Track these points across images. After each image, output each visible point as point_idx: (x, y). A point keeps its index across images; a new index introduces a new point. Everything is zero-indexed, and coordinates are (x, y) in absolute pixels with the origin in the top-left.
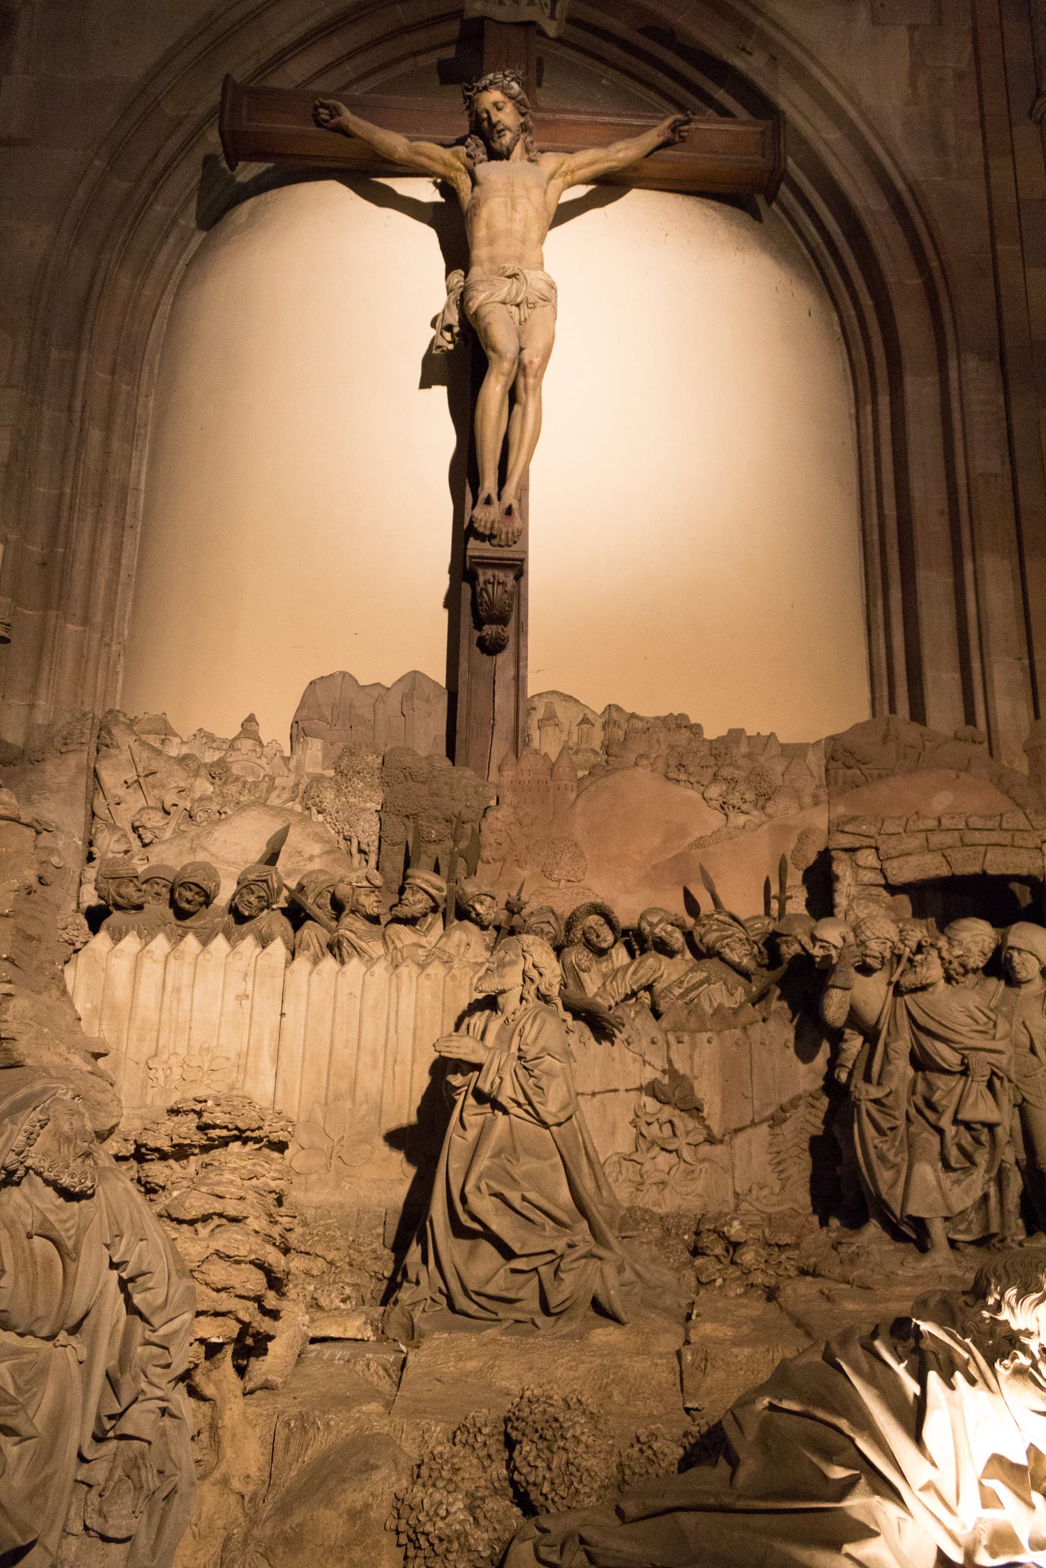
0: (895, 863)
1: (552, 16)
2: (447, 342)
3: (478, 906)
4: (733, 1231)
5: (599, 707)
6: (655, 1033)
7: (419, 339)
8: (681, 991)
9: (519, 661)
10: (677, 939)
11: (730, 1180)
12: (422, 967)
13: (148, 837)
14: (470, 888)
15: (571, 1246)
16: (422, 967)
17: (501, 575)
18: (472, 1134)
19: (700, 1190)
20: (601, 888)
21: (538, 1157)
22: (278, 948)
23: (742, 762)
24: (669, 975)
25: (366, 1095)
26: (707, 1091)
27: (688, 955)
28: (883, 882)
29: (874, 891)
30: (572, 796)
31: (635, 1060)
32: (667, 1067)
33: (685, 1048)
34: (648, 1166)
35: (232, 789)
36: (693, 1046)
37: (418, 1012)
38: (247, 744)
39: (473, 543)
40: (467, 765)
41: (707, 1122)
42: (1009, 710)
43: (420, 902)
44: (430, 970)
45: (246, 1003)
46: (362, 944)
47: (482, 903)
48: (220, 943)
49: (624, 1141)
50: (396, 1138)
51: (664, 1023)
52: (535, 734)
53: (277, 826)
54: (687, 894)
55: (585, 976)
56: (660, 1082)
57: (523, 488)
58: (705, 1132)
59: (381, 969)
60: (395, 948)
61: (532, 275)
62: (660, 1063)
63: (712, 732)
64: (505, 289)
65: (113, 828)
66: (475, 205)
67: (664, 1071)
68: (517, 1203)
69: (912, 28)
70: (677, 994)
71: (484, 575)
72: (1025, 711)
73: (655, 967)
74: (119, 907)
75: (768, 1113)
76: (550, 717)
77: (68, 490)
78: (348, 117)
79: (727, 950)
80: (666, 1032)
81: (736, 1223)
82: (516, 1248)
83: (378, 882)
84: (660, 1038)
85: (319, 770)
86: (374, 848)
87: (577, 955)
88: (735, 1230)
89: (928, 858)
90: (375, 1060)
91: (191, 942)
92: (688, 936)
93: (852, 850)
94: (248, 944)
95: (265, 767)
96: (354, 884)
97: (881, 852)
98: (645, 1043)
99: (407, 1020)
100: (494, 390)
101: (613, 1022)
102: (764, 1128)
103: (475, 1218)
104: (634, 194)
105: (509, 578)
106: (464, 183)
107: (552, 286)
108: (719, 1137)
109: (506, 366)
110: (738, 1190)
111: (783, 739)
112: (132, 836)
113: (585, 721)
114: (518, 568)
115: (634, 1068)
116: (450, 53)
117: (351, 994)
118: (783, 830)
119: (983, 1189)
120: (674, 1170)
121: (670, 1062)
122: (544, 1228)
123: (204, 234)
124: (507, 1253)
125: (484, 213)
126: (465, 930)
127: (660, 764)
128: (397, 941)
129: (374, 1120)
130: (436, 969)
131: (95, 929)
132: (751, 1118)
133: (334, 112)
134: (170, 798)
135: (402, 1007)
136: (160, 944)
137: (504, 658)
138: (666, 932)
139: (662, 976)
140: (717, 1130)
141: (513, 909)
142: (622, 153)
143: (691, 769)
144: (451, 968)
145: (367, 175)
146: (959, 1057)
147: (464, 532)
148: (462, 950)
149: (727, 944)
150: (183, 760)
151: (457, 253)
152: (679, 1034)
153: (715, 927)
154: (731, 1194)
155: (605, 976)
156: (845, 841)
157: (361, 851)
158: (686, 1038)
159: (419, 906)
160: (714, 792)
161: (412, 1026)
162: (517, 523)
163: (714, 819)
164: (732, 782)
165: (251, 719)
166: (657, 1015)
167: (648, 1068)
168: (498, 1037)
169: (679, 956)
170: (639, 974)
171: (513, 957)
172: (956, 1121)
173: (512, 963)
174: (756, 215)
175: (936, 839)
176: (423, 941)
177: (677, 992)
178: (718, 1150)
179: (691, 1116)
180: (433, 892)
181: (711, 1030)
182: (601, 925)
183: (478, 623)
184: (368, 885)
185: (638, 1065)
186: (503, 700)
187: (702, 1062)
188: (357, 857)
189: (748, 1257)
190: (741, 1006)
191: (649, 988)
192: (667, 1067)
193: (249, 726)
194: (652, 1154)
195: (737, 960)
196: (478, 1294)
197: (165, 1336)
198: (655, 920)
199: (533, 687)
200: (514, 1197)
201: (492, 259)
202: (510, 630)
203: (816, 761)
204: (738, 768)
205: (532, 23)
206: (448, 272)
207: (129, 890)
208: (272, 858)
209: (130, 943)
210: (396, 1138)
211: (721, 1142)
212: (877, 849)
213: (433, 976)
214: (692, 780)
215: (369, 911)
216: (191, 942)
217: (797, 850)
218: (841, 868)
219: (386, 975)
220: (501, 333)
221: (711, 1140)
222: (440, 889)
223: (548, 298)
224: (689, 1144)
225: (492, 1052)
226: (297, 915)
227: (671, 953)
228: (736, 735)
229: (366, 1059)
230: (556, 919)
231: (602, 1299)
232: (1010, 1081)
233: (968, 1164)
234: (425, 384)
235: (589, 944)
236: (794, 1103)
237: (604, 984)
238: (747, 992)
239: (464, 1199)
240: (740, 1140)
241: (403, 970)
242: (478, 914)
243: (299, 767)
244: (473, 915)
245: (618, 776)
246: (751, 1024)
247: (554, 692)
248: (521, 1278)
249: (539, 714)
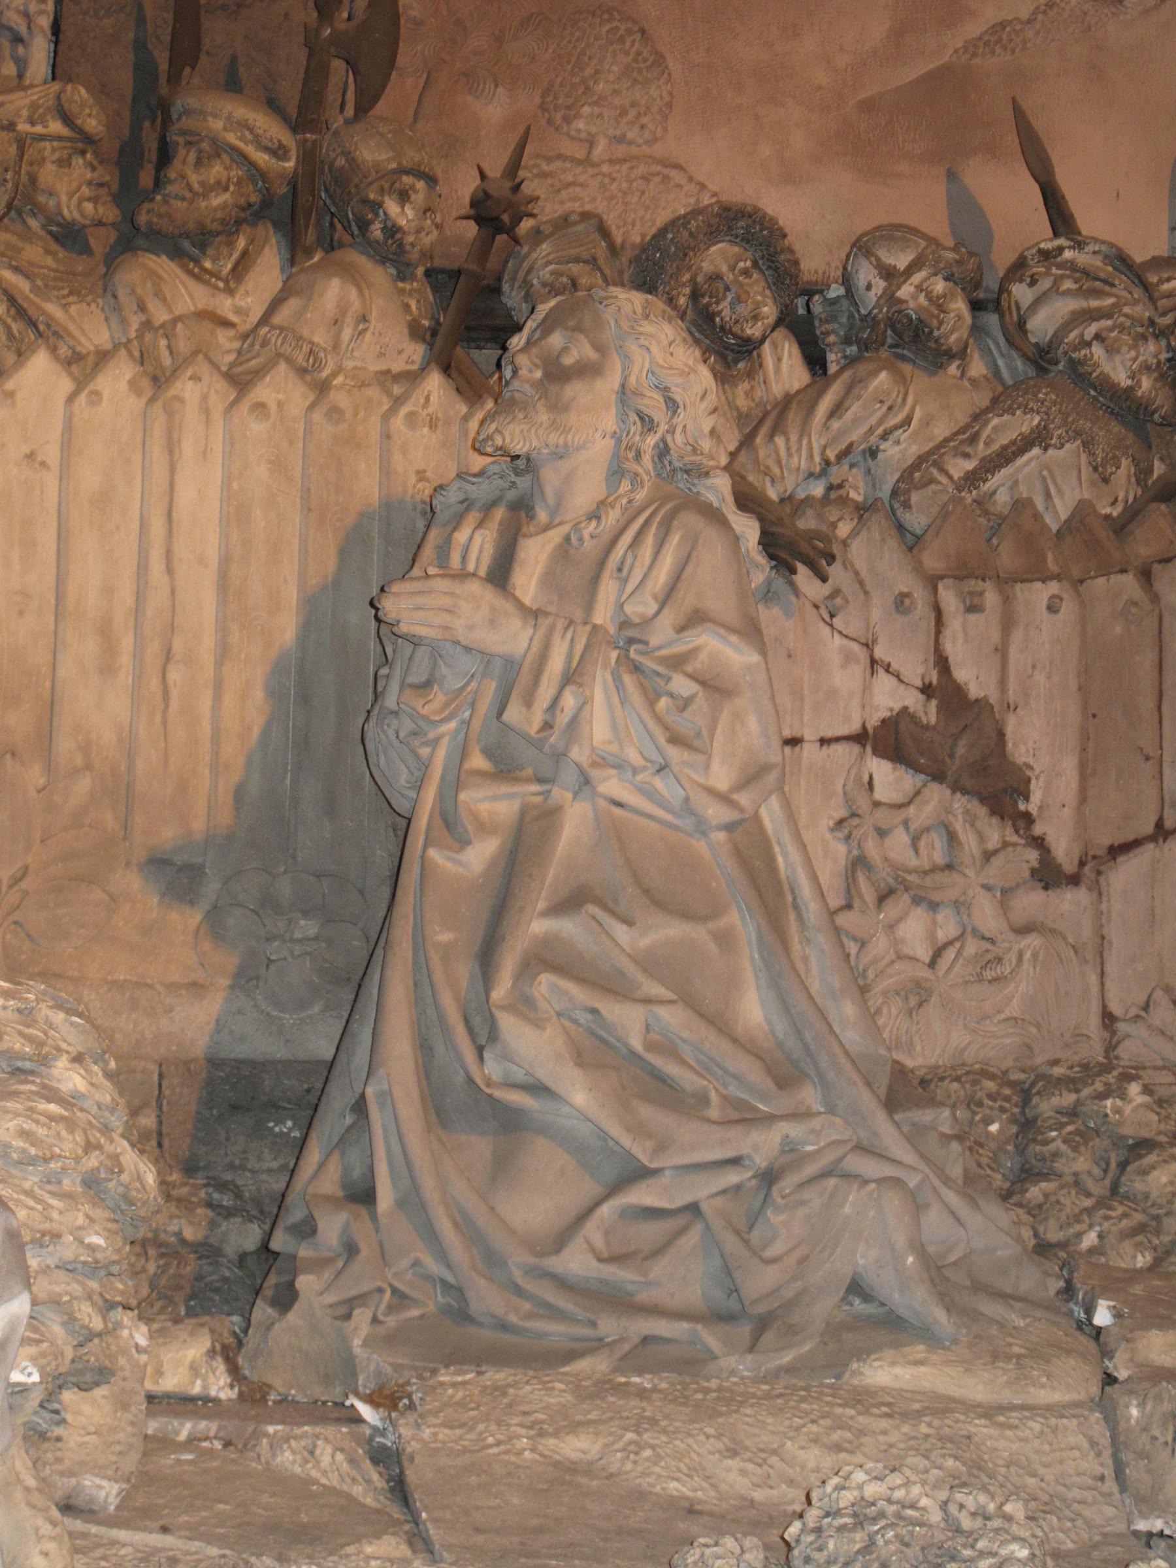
3: (392, 207)
6: (905, 582)
8: (969, 465)
11: (1093, 979)
12: (241, 381)
14: (372, 152)
16: (241, 381)
18: (480, 854)
19: (1014, 1008)
20: (716, 166)
21: (686, 915)
24: (927, 422)
25: (86, 749)
26: (1040, 742)
31: (848, 658)
32: (934, 677)
36: (1008, 623)
37: (236, 513)
41: (1038, 829)
44: (264, 392)
46: (53, 309)
47: (404, 197)
50: (177, 875)
56: (913, 718)
58: (1033, 856)
59: (117, 382)
60: (147, 325)
62: (915, 666)
67: (927, 690)
70: (957, 475)
79: (1097, 351)
80: (933, 582)
83: (92, 124)
84: (920, 595)
90: (109, 649)
96: (23, 127)
99: (201, 537)
101: (804, 546)
108: (1069, 867)
110: (1116, 1008)
115: (846, 678)
117: (31, 456)
120: (950, 954)
121: (943, 663)
126: (350, 273)
128: (152, 305)
129: (110, 820)
130: (279, 389)
132: (1153, 820)
135: (186, 496)
138: (929, 297)
139: (908, 421)
140: (1064, 850)
141: (495, 215)
144: (322, 388)
149: (1098, 337)
152: (972, 584)
153: (1068, 285)
158: (991, 598)
159: (217, 200)
161: (213, 555)
167: (884, 681)
168: (549, 579)
169: (953, 369)
170: (849, 415)
171: (591, 354)
173: (587, 371)
176: (225, 306)
177: (960, 467)
181: (1058, 577)
182: (746, 272)
184: (65, 131)
185: (858, 670)
190: (1133, 513)
192: (934, 677)
194: (892, 909)
195: (1122, 378)
198: (901, 261)
211: (1074, 880)
213: (273, 408)
215: (70, 212)
219: (135, 404)
221: (1048, 875)
222: (279, 152)
225: (545, 623)
229: (83, 648)
230: (613, 250)
237: (747, 441)
238: (1142, 473)
240: (1125, 875)
241: (187, 390)
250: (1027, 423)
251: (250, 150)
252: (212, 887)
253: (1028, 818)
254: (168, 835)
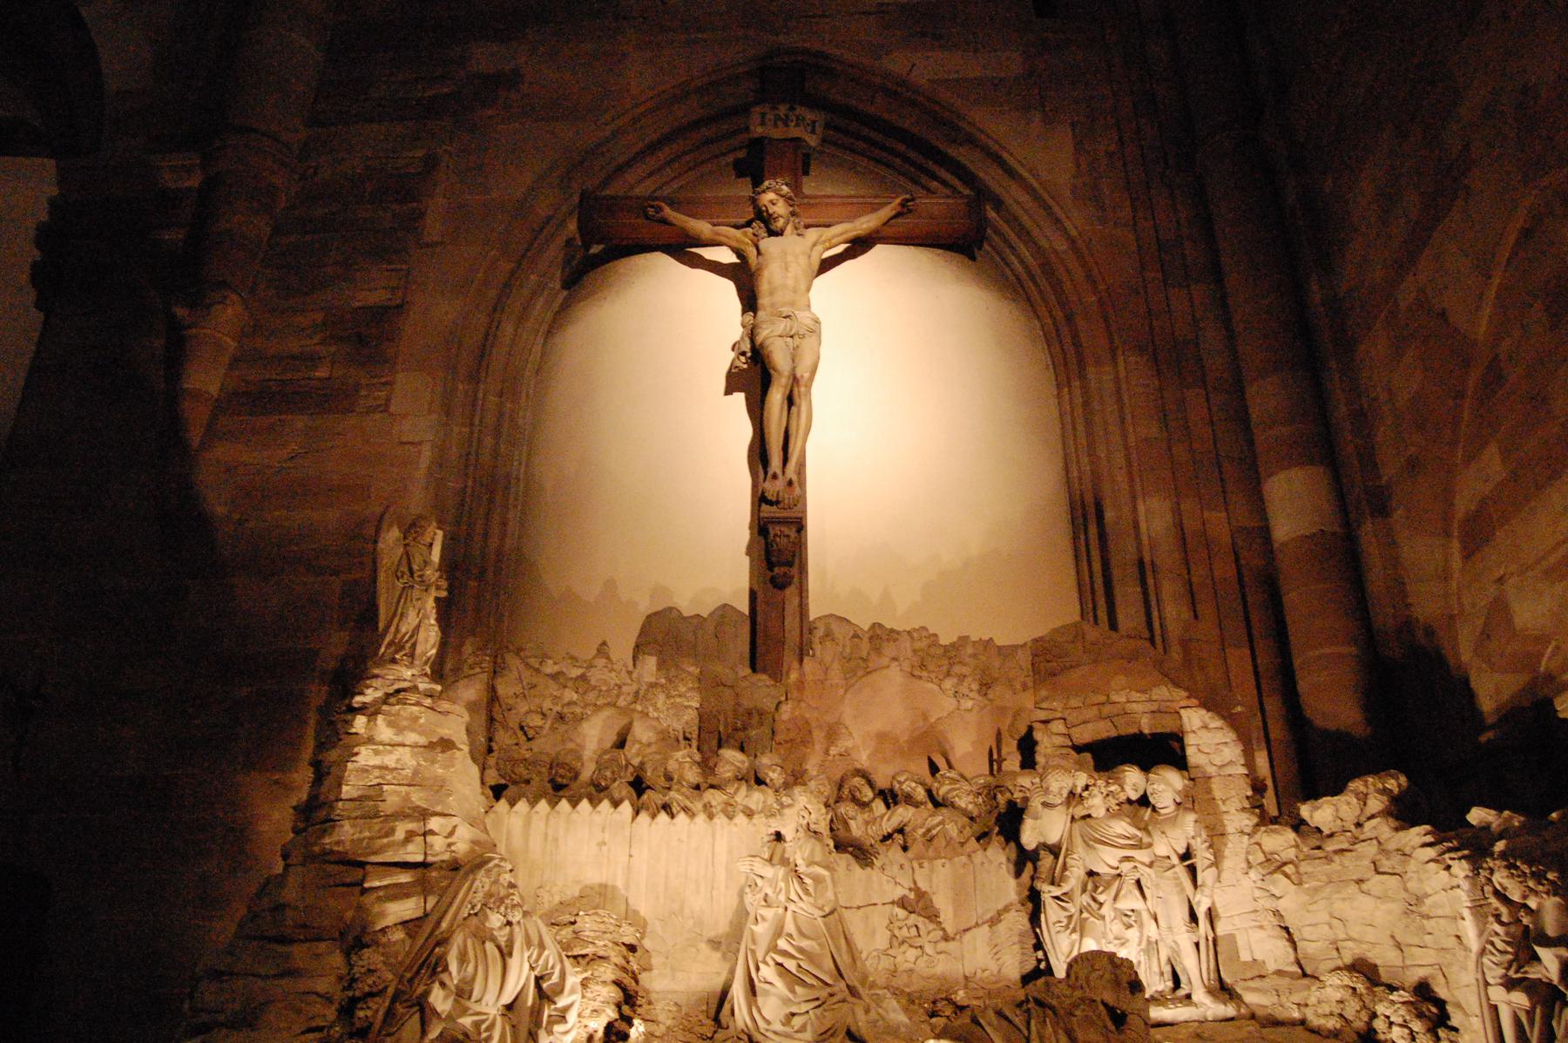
1: (813, 132)
2: (742, 363)
5: (866, 628)
7: (725, 359)
9: (802, 592)
10: (920, 794)
13: (531, 733)
15: (831, 995)
17: (786, 531)
22: (626, 808)
23: (967, 660)
26: (942, 902)
27: (930, 805)
29: (1064, 751)
30: (842, 691)
33: (925, 871)
34: (900, 959)
35: (591, 696)
36: (932, 870)
38: (601, 662)
39: (764, 507)
40: (764, 671)
42: (1173, 612)
44: (736, 820)
45: (604, 848)
48: (585, 804)
49: (881, 940)
50: (715, 944)
51: (910, 854)
52: (817, 647)
53: (625, 721)
54: (930, 760)
55: (852, 823)
57: (801, 466)
59: (701, 818)
61: (803, 316)
63: (945, 640)
64: (782, 326)
65: (506, 727)
66: (760, 269)
69: (1073, 125)
71: (774, 530)
72: (1186, 615)
73: (903, 813)
74: (515, 783)
75: (988, 917)
76: (828, 635)
77: (470, 483)
78: (668, 212)
80: (911, 861)
81: (961, 993)
85: (653, 680)
86: (695, 736)
87: (846, 809)
88: (960, 996)
89: (1102, 724)
91: (564, 805)
92: (929, 792)
93: (1046, 722)
94: (605, 805)
95: (613, 678)
98: (896, 868)
100: (776, 397)
102: (986, 928)
104: (879, 247)
105: (793, 534)
106: (751, 252)
107: (817, 322)
109: (784, 381)
111: (999, 642)
112: (520, 733)
113: (856, 636)
114: (800, 525)
115: (888, 887)
116: (741, 154)
118: (1002, 710)
123: (565, 293)
125: (766, 274)
127: (906, 666)
131: (497, 797)
133: (661, 209)
134: (547, 705)
136: (543, 805)
137: (791, 592)
140: (950, 931)
142: (865, 224)
143: (931, 668)
145: (683, 249)
147: (760, 499)
150: (555, 677)
151: (750, 302)
155: (867, 823)
156: (1043, 715)
157: (686, 739)
158: (926, 864)
160: (948, 684)
162: (797, 491)
163: (949, 703)
164: (962, 677)
165: (604, 643)
166: (905, 848)
173: (789, 806)
174: (973, 258)
175: (1106, 710)
178: (951, 946)
183: (770, 565)
185: (892, 885)
186: (791, 623)
187: (938, 879)
188: (683, 742)
191: (901, 831)
193: (602, 649)
199: (814, 612)
201: (773, 305)
202: (794, 571)
203: (1024, 658)
204: (965, 665)
205: (798, 139)
206: (744, 312)
207: (521, 770)
208: (621, 744)
209: (522, 806)
210: (715, 944)
216: (564, 805)
217: (1012, 724)
218: (1038, 735)
220: (780, 358)
221: (946, 938)
223: (815, 329)
226: (639, 786)
227: (917, 805)
228: (964, 640)
231: (853, 1029)
234: (728, 392)
235: (854, 800)
236: (1006, 909)
240: (968, 935)
241: (716, 820)
243: (640, 675)
245: (875, 675)
247: (831, 615)
249: (820, 633)
252: (723, 947)
254: (712, 934)
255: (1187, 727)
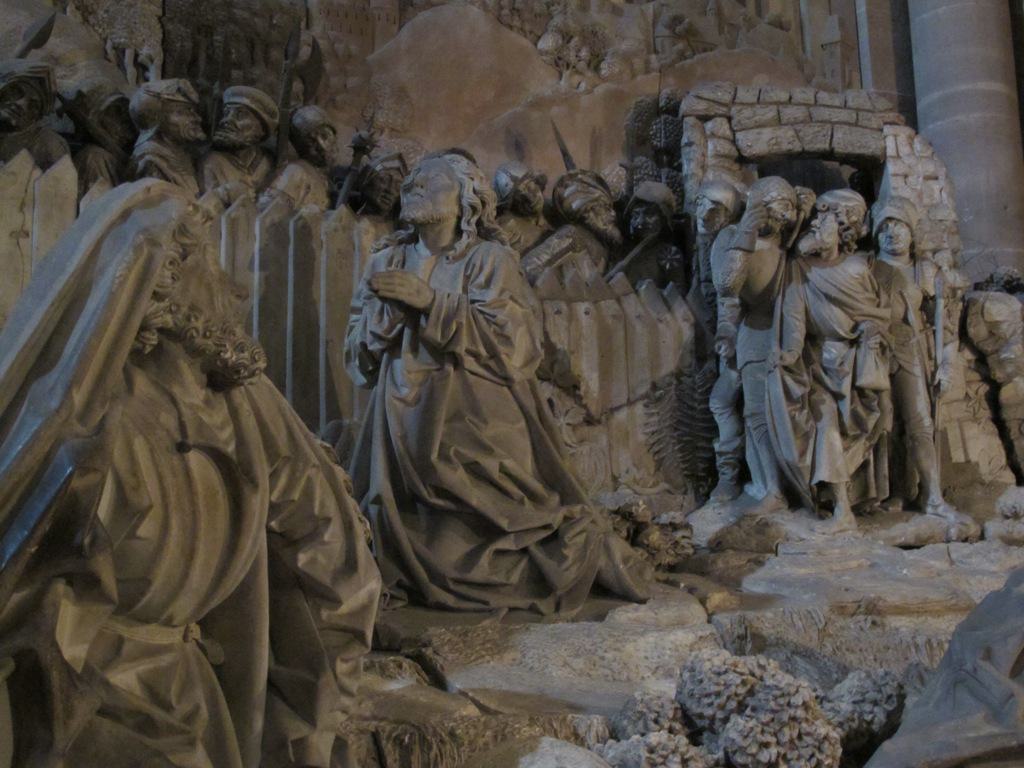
0: (752, 135)
3: (321, 141)
4: (640, 510)
11: (608, 461)
28: (736, 154)
41: (584, 402)
43: (248, 127)
58: (584, 411)
68: (496, 475)
79: (592, 214)
82: (504, 524)
97: (734, 122)
103: (442, 492)
119: (864, 456)
122: (521, 502)
124: (485, 530)
140: (594, 409)
146: (852, 323)
148: (302, 193)
149: (592, 209)
154: (609, 479)
159: (247, 133)
172: (854, 386)
178: (596, 430)
179: (568, 394)
180: (265, 116)
184: (186, 100)
189: (655, 537)
195: (600, 225)
196: (458, 582)
197: (352, 615)
200: (491, 465)
211: (599, 422)
212: (730, 119)
214: (527, 27)
221: (589, 421)
222: (272, 115)
224: (568, 424)
231: (609, 577)
232: (891, 350)
233: (858, 432)
239: (426, 470)
242: (320, 149)
244: (314, 152)
246: (626, 295)
248: (506, 562)
250: (567, 242)
251: (261, 112)
253: (580, 398)
255: (891, 151)
